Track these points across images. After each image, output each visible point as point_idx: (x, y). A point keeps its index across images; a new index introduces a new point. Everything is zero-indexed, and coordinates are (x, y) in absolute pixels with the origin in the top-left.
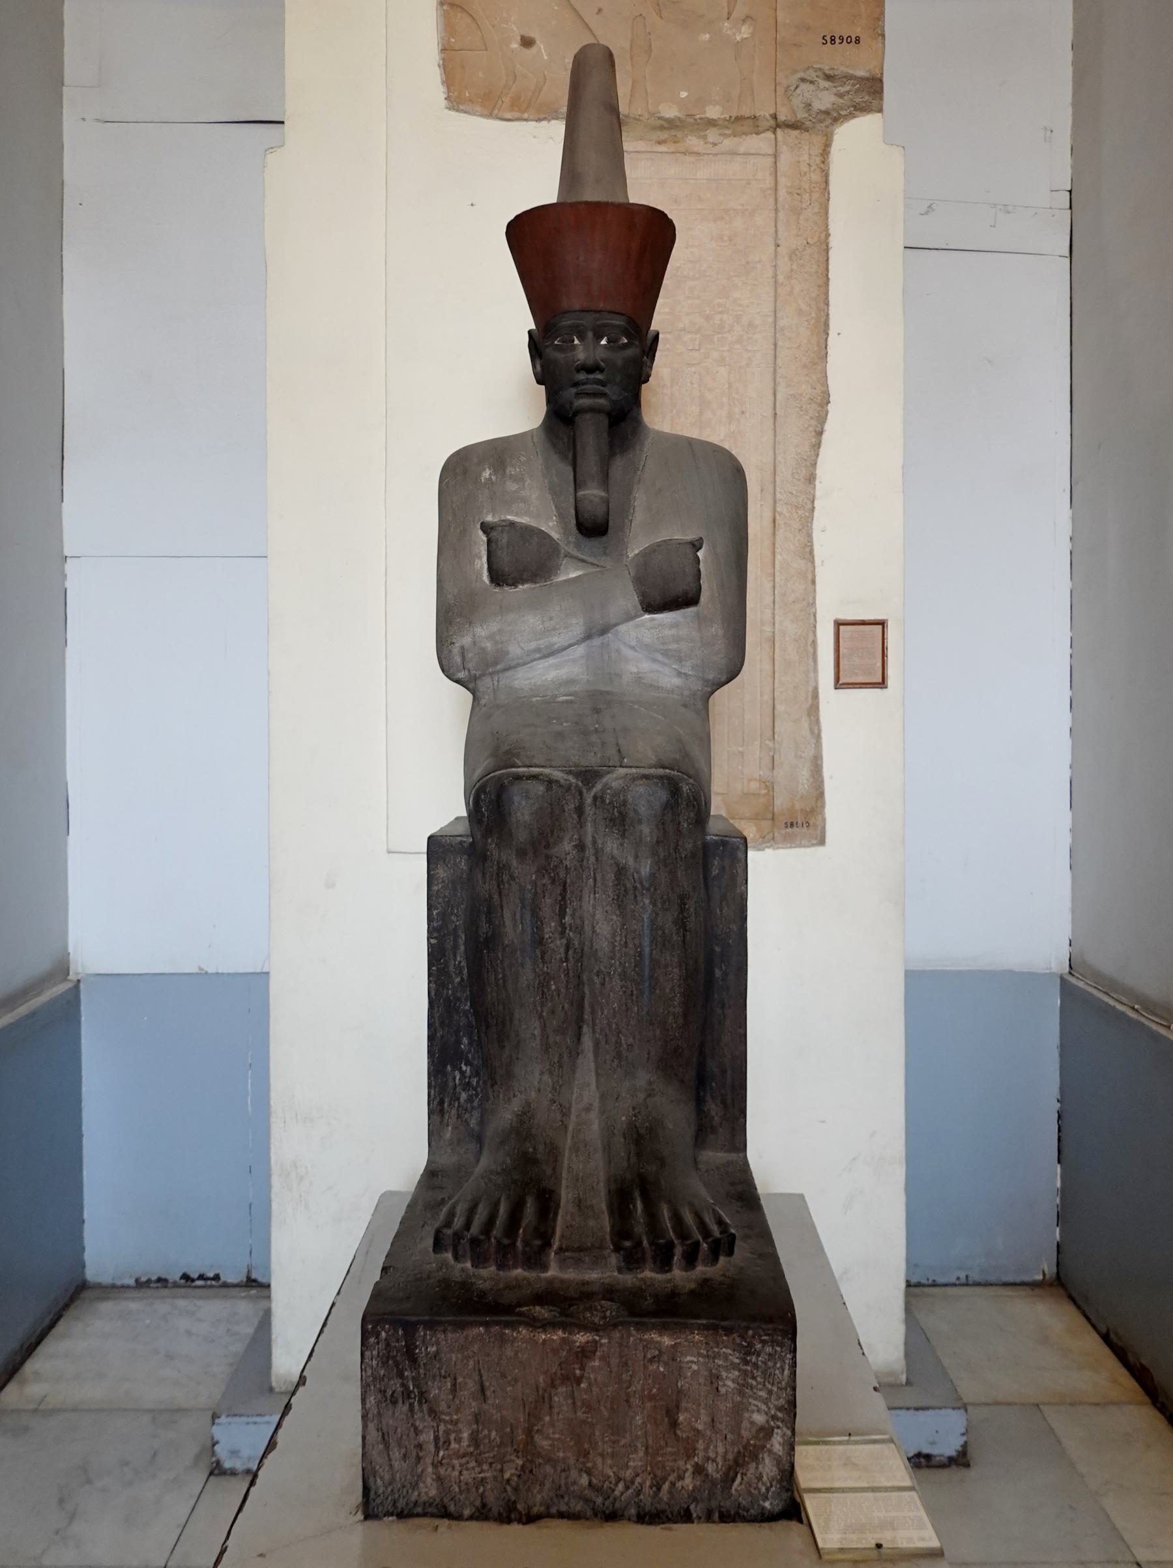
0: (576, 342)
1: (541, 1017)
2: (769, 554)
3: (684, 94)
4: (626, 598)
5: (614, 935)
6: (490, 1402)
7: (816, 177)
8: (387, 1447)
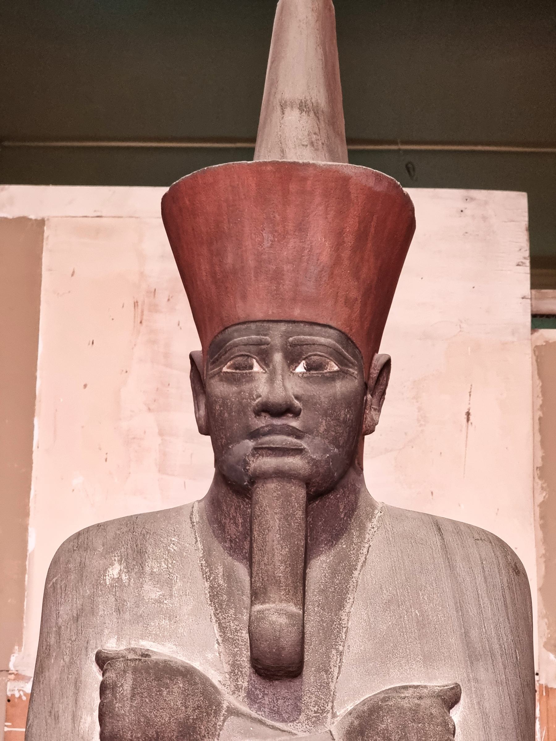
0: (257, 368)
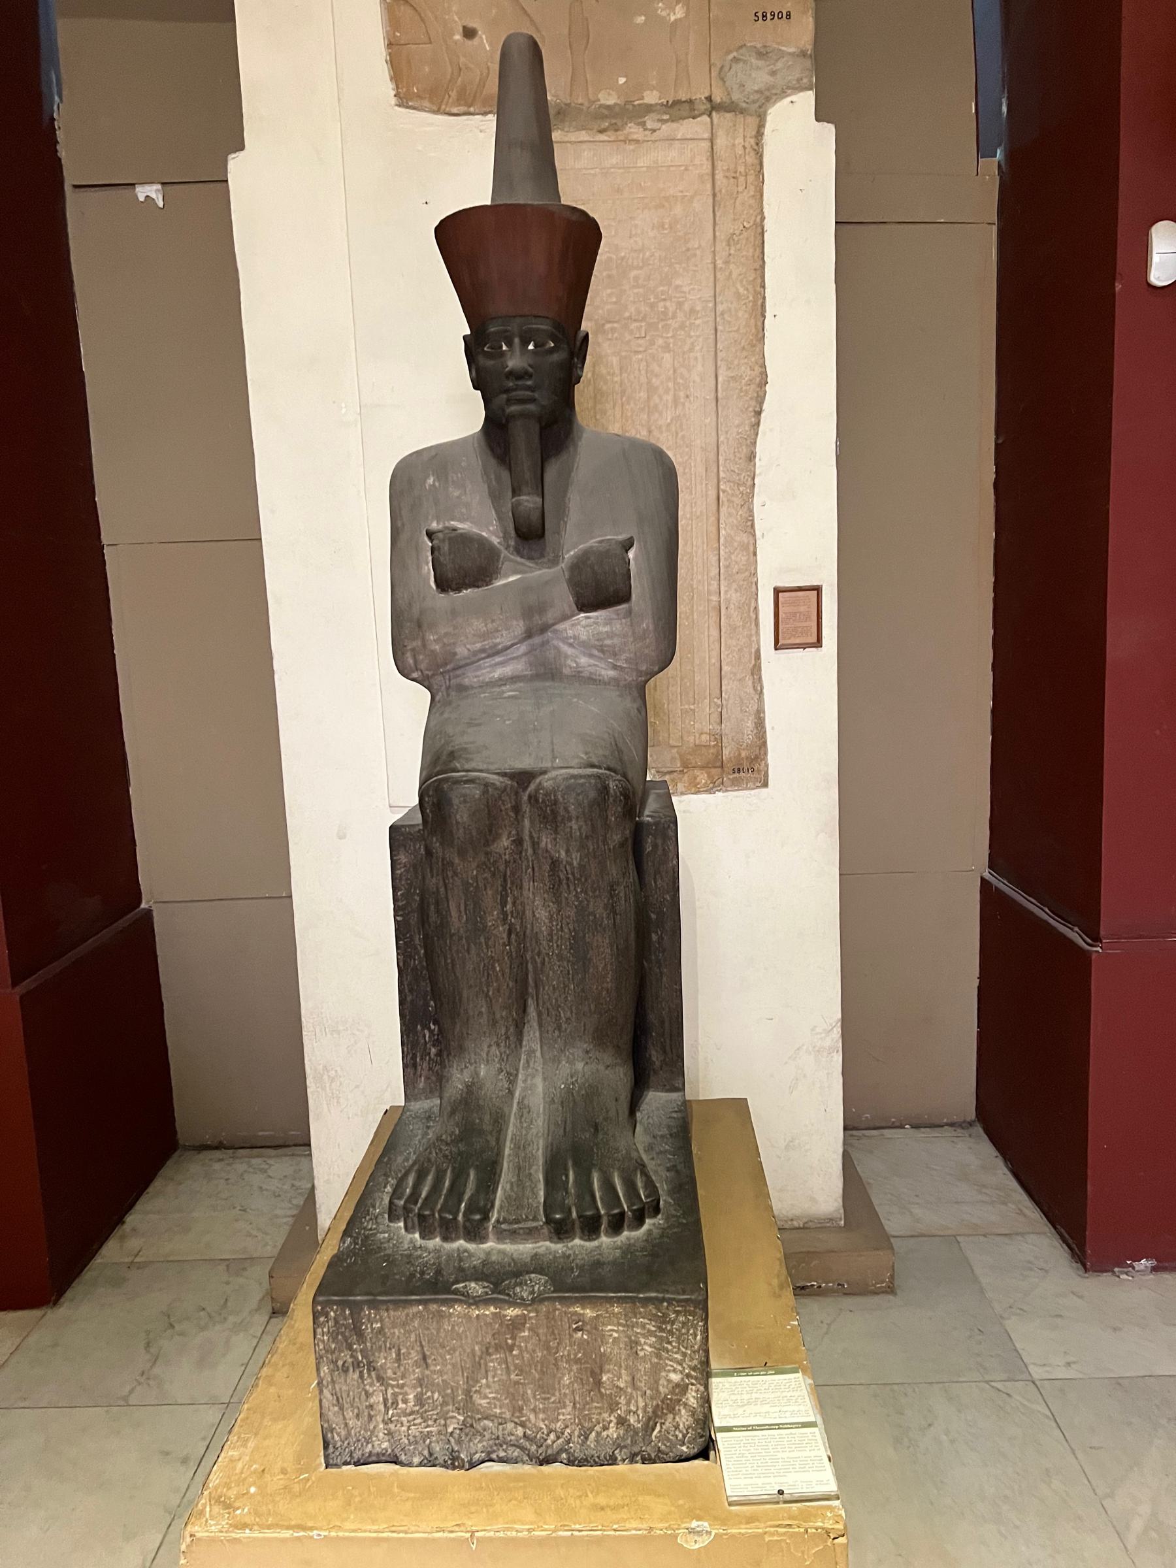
1: (487, 995)
2: (714, 529)
3: (622, 80)
4: (564, 597)
5: (551, 918)
6: (432, 1368)
7: (751, 159)
8: (342, 1409)
